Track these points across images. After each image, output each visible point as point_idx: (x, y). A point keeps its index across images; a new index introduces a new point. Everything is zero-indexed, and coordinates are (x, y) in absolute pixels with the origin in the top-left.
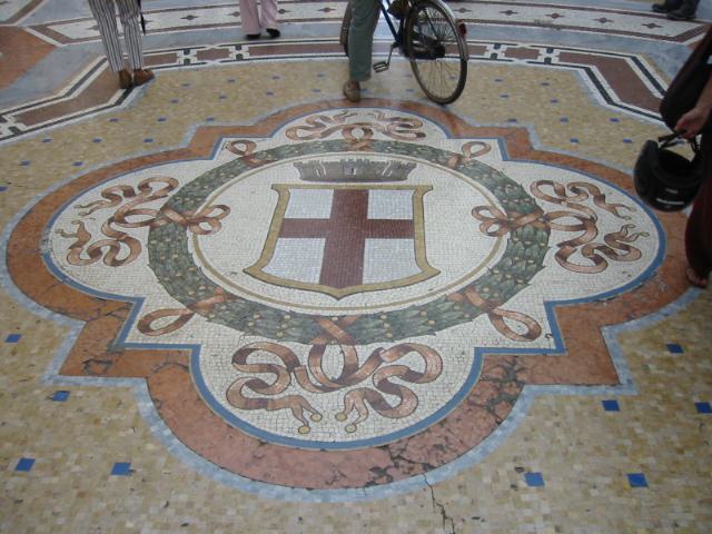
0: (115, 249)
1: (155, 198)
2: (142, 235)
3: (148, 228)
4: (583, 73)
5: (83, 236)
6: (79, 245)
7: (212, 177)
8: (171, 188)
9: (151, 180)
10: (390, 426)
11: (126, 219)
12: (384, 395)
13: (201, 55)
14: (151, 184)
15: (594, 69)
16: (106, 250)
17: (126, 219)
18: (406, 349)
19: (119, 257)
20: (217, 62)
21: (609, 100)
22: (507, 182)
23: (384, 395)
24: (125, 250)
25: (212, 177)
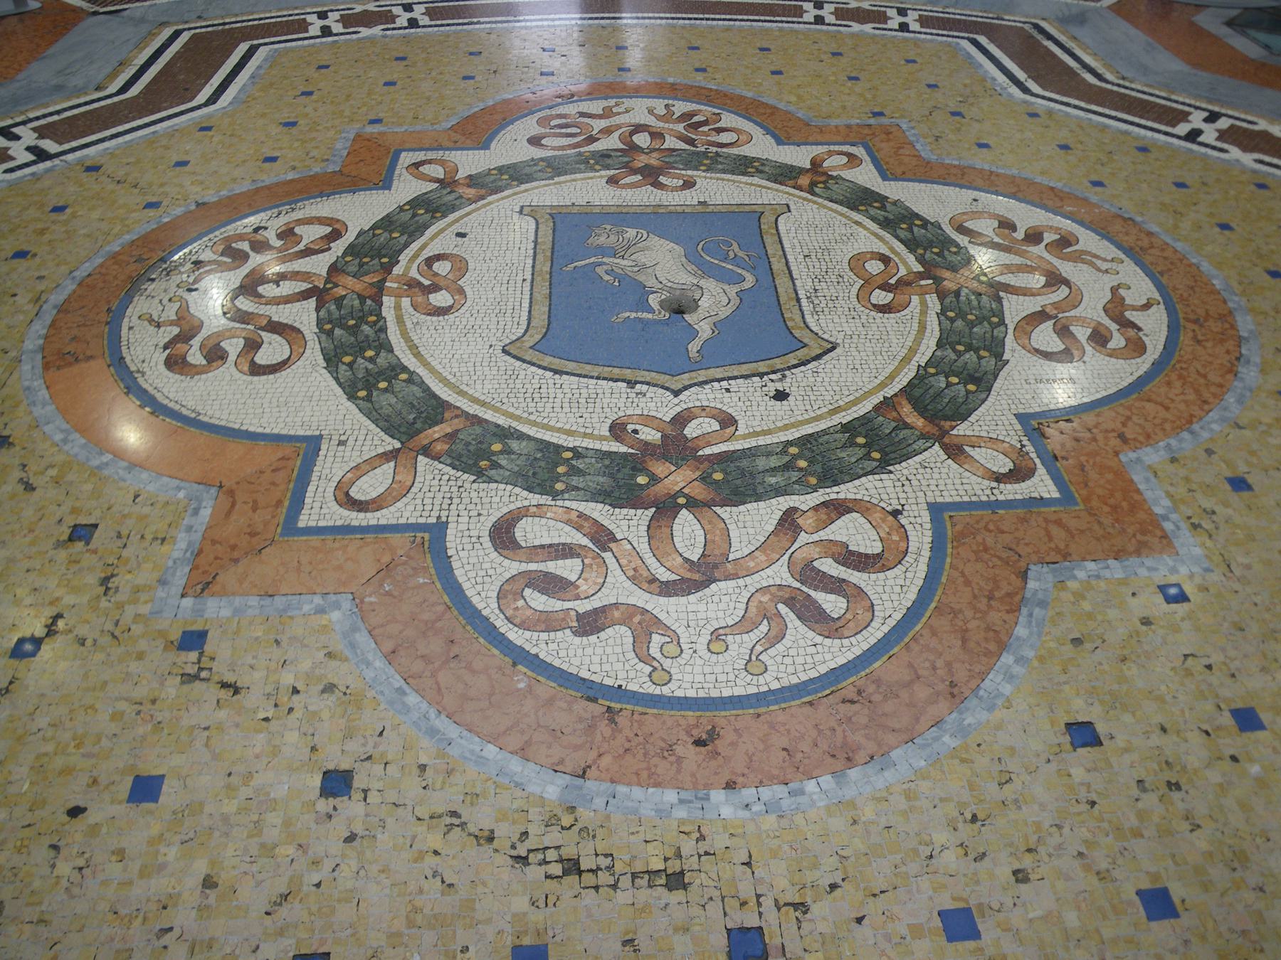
0: (253, 345)
1: (308, 252)
2: (304, 316)
3: (312, 303)
4: (966, 44)
5: (187, 329)
6: (185, 337)
7: (406, 217)
8: (335, 235)
9: (300, 222)
10: (837, 653)
11: (260, 289)
12: (812, 593)
13: (347, 21)
14: (297, 230)
15: (982, 40)
16: (233, 347)
17: (260, 289)
18: (839, 508)
19: (262, 358)
20: (377, 30)
21: (1025, 90)
22: (911, 217)
23: (812, 593)
24: (273, 349)
25: (406, 217)
